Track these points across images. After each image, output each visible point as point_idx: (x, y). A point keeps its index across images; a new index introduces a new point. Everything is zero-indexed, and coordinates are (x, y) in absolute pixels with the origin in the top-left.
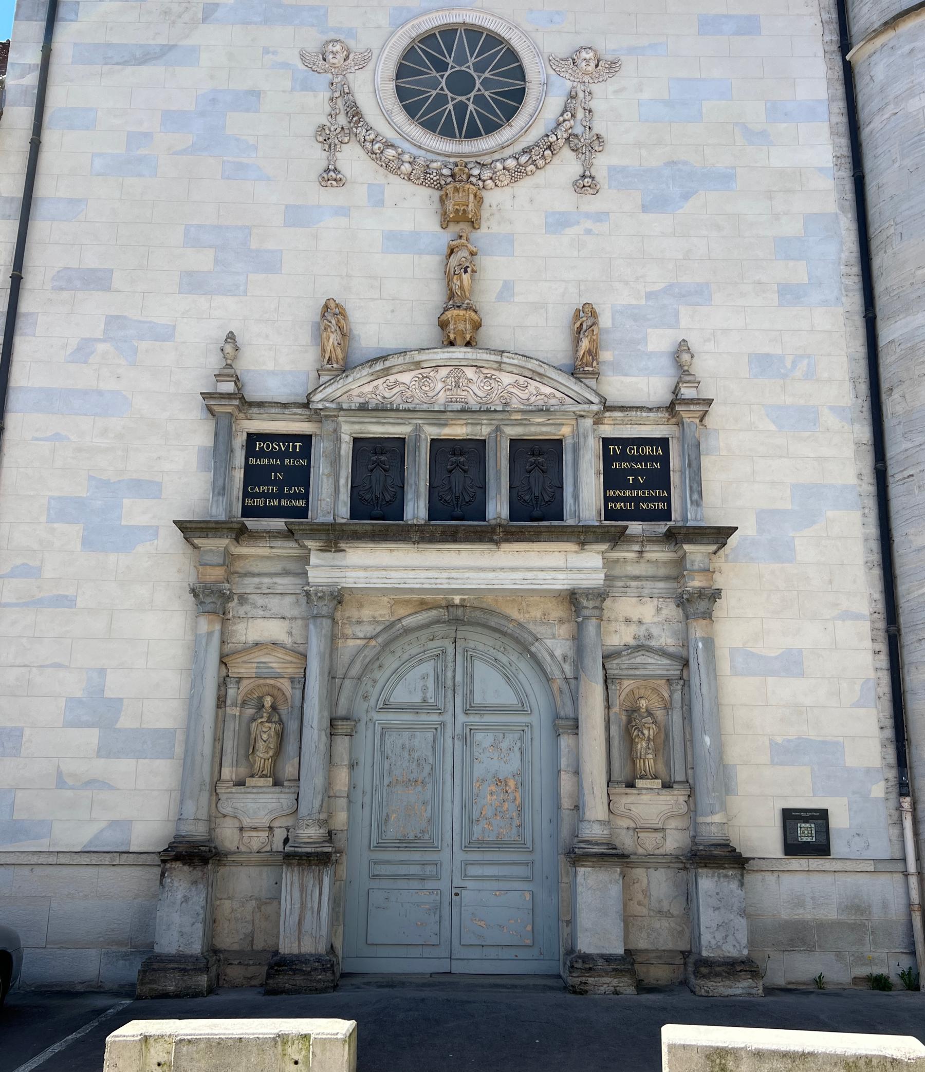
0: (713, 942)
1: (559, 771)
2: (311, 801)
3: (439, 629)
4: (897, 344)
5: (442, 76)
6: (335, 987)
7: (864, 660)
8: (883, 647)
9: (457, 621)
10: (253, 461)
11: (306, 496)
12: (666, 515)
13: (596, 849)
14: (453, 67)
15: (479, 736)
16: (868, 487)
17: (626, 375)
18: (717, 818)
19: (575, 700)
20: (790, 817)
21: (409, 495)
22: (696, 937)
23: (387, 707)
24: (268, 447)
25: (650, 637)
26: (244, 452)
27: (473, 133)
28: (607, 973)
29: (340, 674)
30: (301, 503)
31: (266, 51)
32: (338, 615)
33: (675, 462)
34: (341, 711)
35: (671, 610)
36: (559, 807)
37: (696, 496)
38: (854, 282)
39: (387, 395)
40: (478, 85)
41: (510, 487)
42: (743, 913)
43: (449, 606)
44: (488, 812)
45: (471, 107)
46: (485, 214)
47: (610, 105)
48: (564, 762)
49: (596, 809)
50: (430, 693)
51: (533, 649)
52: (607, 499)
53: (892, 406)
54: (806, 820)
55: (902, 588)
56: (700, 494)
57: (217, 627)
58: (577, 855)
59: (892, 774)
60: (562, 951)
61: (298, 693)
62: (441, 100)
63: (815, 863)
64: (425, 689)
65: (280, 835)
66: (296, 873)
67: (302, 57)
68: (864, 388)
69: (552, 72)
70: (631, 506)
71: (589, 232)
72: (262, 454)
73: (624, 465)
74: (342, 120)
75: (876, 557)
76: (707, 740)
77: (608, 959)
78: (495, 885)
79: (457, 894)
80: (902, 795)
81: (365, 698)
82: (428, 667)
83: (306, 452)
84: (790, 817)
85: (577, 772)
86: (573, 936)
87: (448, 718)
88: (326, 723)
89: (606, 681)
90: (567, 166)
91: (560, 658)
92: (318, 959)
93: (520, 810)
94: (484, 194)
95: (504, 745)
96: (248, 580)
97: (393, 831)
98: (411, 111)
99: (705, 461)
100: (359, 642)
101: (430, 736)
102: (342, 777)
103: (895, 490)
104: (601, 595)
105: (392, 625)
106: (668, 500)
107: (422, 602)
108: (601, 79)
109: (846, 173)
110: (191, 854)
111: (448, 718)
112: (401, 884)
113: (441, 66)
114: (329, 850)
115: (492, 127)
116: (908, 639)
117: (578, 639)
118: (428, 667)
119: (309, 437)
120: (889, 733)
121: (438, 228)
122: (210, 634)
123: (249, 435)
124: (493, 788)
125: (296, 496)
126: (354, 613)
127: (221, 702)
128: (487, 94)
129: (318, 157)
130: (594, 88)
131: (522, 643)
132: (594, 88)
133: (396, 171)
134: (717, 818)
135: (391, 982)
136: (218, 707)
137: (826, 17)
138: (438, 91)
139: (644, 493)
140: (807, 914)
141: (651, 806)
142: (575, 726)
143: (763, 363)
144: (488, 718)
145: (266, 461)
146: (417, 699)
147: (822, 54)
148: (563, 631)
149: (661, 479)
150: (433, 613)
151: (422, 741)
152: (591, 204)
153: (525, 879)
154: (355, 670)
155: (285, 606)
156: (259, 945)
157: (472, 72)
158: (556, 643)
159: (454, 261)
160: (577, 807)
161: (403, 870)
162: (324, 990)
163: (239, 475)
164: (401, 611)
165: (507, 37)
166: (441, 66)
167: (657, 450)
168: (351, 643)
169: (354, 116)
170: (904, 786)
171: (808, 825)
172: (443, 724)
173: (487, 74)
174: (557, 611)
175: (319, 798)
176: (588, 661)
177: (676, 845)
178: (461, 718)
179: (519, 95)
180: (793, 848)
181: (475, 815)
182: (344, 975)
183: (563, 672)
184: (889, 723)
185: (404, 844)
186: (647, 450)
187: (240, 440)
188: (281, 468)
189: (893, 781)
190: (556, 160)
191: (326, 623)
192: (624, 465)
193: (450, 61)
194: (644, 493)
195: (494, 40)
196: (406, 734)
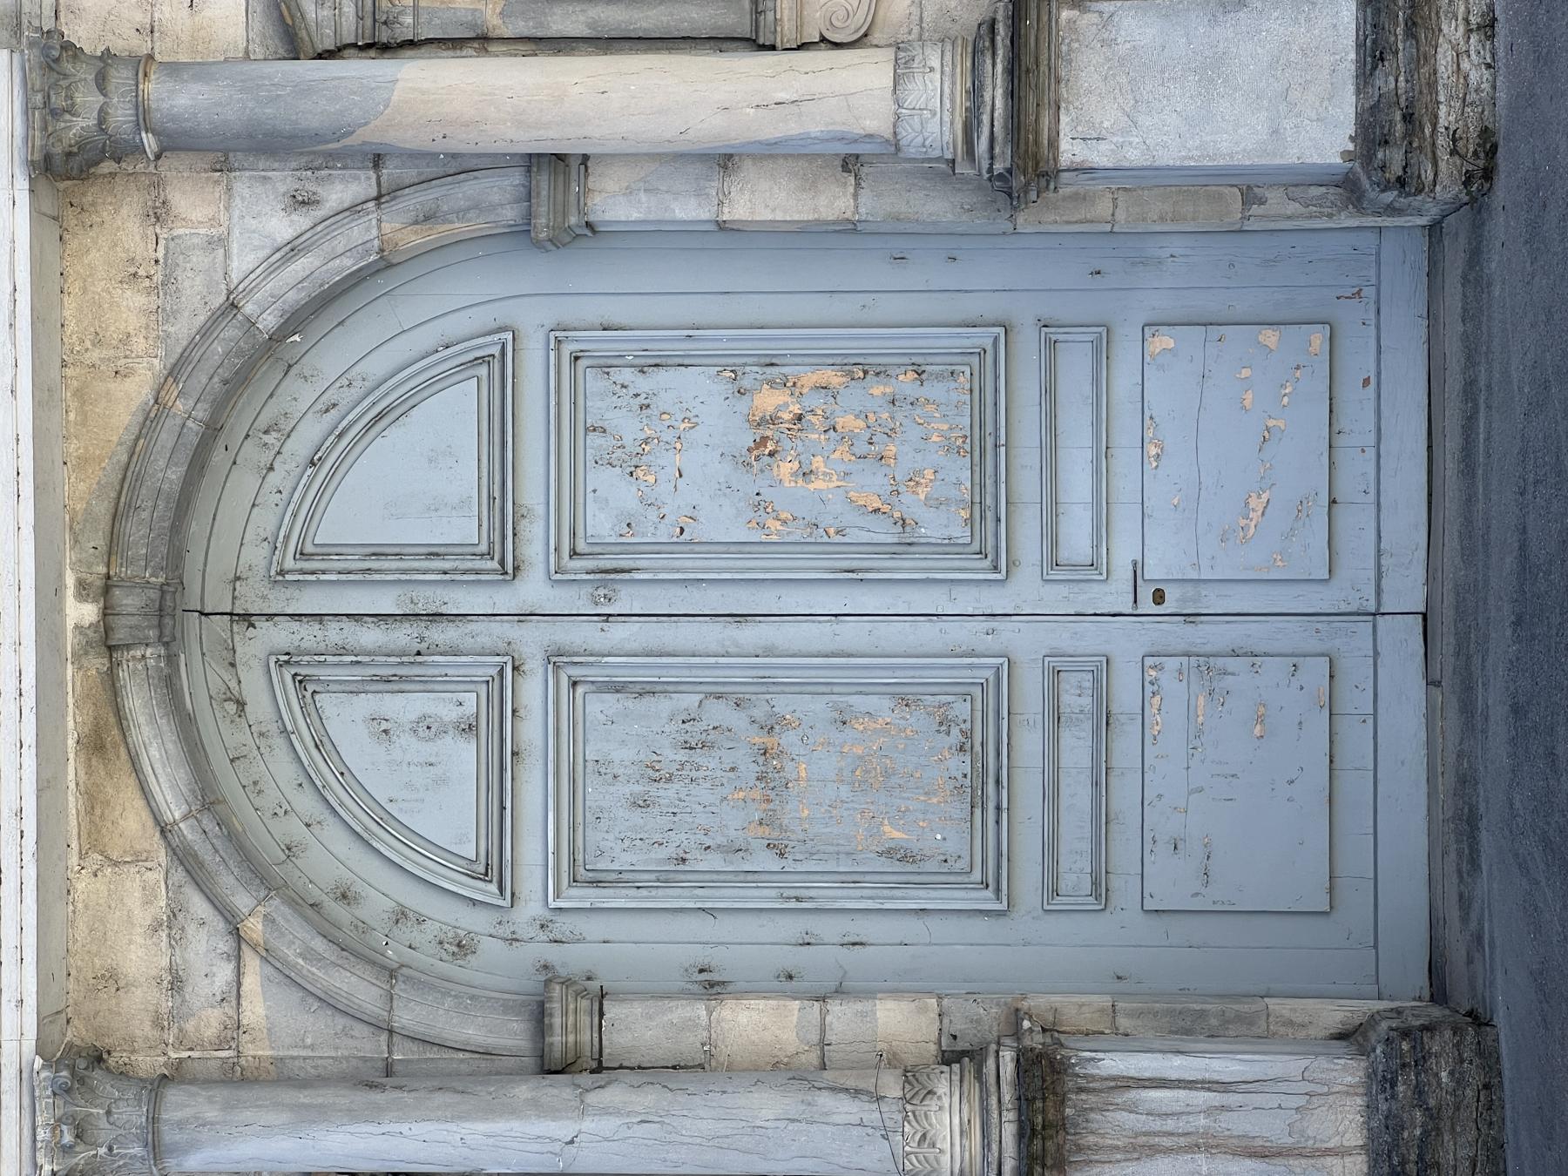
1: (722, 226)
3: (201, 678)
6: (1478, 1020)
9: (168, 614)
13: (996, 95)
15: (600, 524)
19: (461, 166)
23: (494, 868)
28: (1423, 59)
29: (371, 1046)
32: (148, 1063)
34: (513, 1034)
36: (850, 228)
43: (107, 641)
44: (870, 486)
48: (689, 209)
49: (849, 93)
50: (444, 708)
51: (269, 322)
58: (1017, 166)
60: (1348, 220)
64: (426, 727)
78: (1125, 460)
79: (1159, 597)
81: (463, 948)
82: (346, 718)
85: (725, 161)
86: (1297, 181)
87: (532, 641)
88: (558, 1090)
89: (384, 49)
91: (302, 221)
92: (1382, 1083)
93: (862, 369)
95: (629, 428)
97: (942, 831)
100: (251, 982)
101: (599, 706)
102: (751, 1023)
105: (183, 857)
107: (95, 745)
111: (532, 641)
112: (1124, 795)
114: (1008, 1056)
117: (227, 152)
118: (346, 718)
124: (786, 468)
126: (138, 1006)
131: (245, 364)
135: (1459, 825)
142: (555, 169)
144: (532, 492)
146: (463, 757)
148: (194, 204)
150: (138, 701)
151: (621, 735)
153: (1103, 350)
154: (361, 990)
158: (245, 235)
160: (850, 164)
161: (1077, 795)
162: (1489, 1059)
164: (132, 823)
168: (255, 1010)
172: (556, 658)
174: (119, 227)
175: (825, 1100)
176: (313, 114)
178: (533, 590)
181: (885, 533)
182: (1438, 993)
183: (354, 209)
185: (986, 791)
191: (179, 1105)
196: (595, 793)
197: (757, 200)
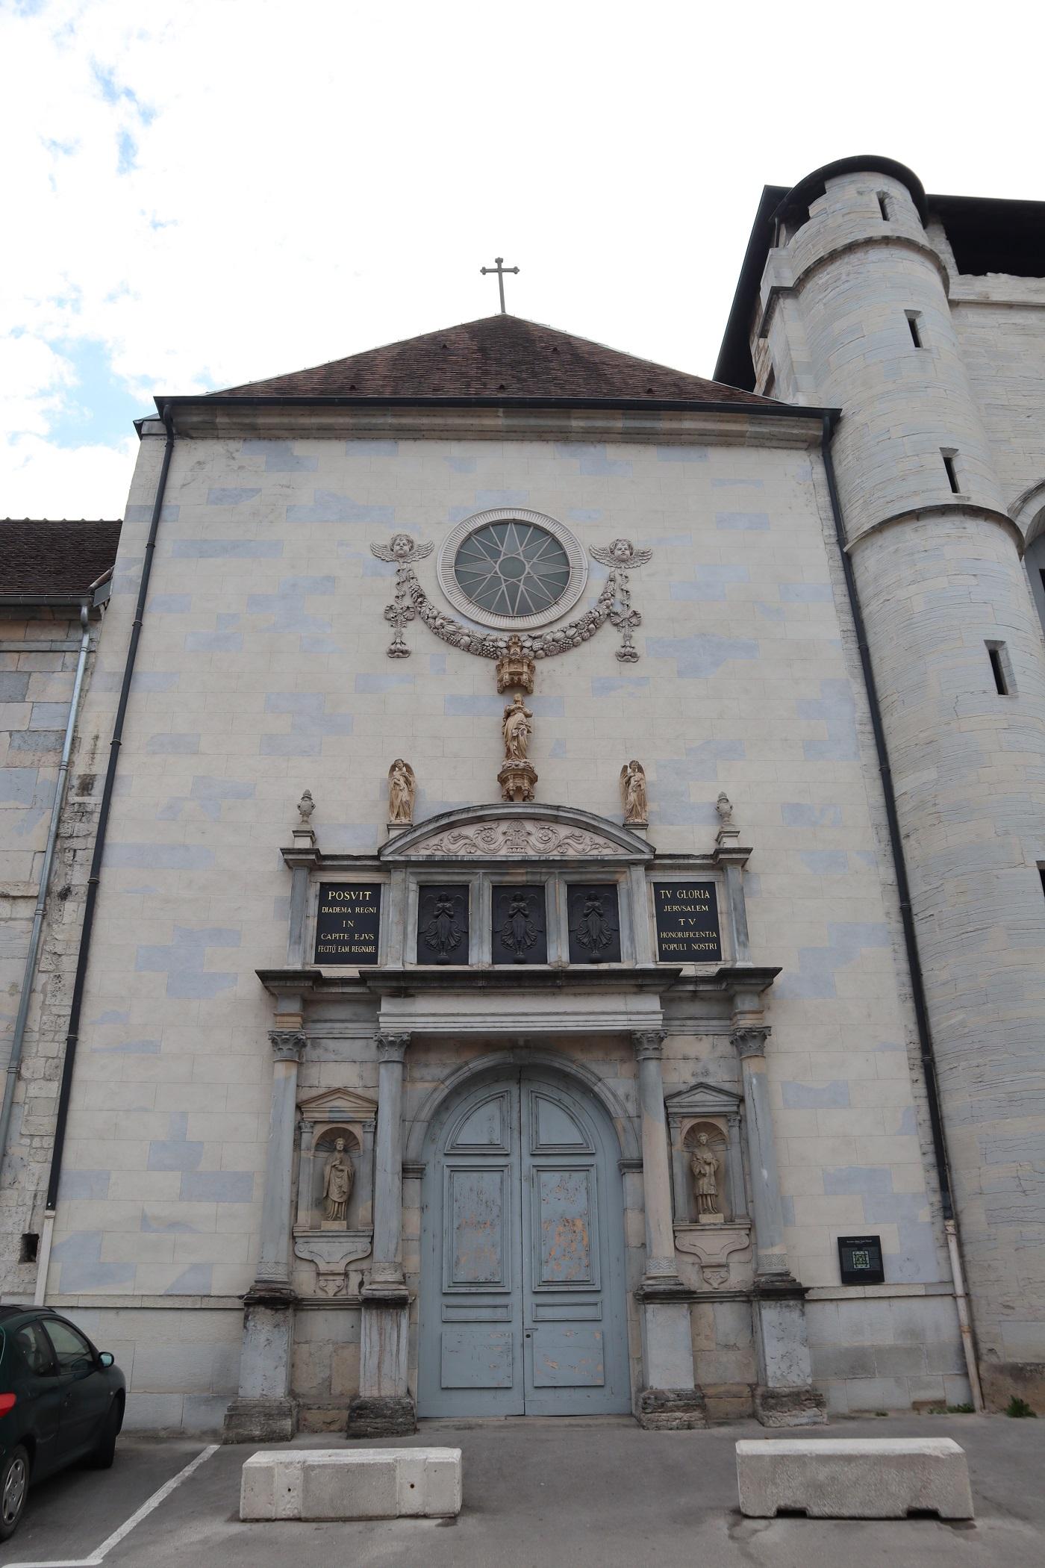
0: (779, 1373)
1: (625, 1210)
2: (385, 1244)
7: (903, 1087)
8: (919, 1074)
10: (325, 910)
11: (375, 943)
12: (716, 955)
16: (897, 926)
18: (776, 1250)
19: (638, 1138)
20: (845, 1244)
21: (474, 941)
22: (762, 1370)
25: (706, 1073)
27: (524, 612)
29: (409, 1116)
30: (370, 949)
33: (722, 905)
35: (724, 1045)
37: (742, 938)
38: (869, 740)
39: (451, 847)
40: (527, 569)
41: (570, 931)
42: (806, 1342)
45: (522, 587)
47: (645, 588)
48: (629, 1201)
49: (663, 1245)
51: (596, 1089)
52: (661, 941)
53: (911, 849)
54: (860, 1248)
55: (934, 1019)
56: (747, 935)
57: (294, 1071)
59: (936, 1198)
60: (633, 1389)
61: (370, 1136)
62: (495, 580)
63: (870, 1290)
65: (355, 1279)
66: (374, 1317)
67: (373, 549)
68: (885, 833)
72: (334, 903)
73: (675, 908)
74: (408, 602)
75: (908, 990)
76: (765, 1173)
77: (679, 1396)
80: (946, 1218)
83: (375, 901)
84: (845, 1244)
86: (643, 1374)
89: (667, 1118)
90: (609, 639)
91: (622, 1097)
94: (535, 663)
96: (319, 1025)
98: (468, 591)
99: (750, 904)
100: (427, 1085)
103: (920, 928)
104: (659, 1038)
106: (717, 941)
109: (853, 646)
110: (271, 1300)
114: (406, 1293)
115: (542, 606)
116: (942, 1067)
119: (379, 885)
120: (931, 1158)
121: (496, 693)
122: (287, 1079)
124: (561, 1229)
125: (366, 943)
127: (297, 1144)
129: (385, 634)
130: (628, 572)
132: (628, 572)
133: (456, 644)
134: (776, 1250)
136: (295, 1150)
137: (823, 515)
140: (866, 1341)
141: (713, 1243)
142: (638, 1166)
147: (822, 546)
149: (710, 921)
156: (337, 1389)
159: (513, 721)
160: (644, 1245)
163: (313, 923)
166: (495, 554)
170: (948, 1210)
175: (395, 1241)
180: (850, 1277)
181: (544, 1257)
183: (626, 1111)
184: (931, 1148)
186: (696, 893)
188: (352, 916)
189: (938, 1205)
190: (600, 633)
192: (675, 908)
193: (503, 549)
197: (633, 1219)
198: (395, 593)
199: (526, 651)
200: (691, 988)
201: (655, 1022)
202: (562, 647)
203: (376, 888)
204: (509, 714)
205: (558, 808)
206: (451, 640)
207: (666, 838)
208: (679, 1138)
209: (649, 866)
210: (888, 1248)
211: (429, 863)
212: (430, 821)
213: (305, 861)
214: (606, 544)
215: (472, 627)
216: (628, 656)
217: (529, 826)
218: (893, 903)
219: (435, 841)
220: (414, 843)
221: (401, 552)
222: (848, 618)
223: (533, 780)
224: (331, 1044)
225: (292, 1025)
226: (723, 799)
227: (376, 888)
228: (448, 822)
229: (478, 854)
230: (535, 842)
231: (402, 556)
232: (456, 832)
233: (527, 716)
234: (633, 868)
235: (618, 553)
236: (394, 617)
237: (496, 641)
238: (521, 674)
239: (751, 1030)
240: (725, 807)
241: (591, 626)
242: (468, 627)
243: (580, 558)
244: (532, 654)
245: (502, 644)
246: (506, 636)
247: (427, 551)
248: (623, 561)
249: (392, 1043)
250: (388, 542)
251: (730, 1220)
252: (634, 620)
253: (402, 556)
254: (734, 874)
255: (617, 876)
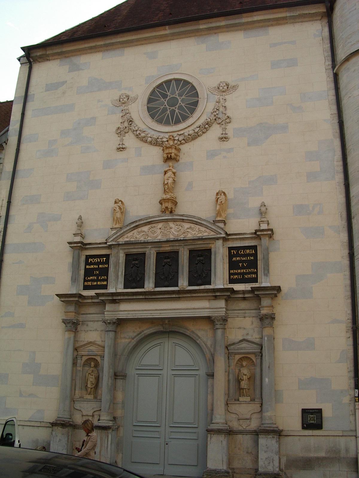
4: (355, 197)
5: (165, 100)
10: (88, 267)
11: (107, 280)
12: (255, 280)
14: (170, 96)
17: (239, 219)
24: (93, 260)
26: (84, 263)
27: (178, 122)
30: (105, 283)
31: (99, 101)
33: (259, 256)
35: (256, 322)
36: (207, 409)
37: (266, 272)
39: (138, 236)
40: (180, 102)
41: (189, 271)
45: (177, 111)
46: (181, 155)
51: (198, 342)
52: (230, 274)
54: (312, 414)
62: (165, 110)
69: (210, 93)
70: (240, 277)
71: (225, 157)
72: (91, 264)
73: (238, 259)
74: (126, 124)
75: (349, 293)
79: (167, 444)
83: (107, 262)
90: (215, 131)
98: (152, 116)
100: (126, 340)
102: (120, 396)
108: (230, 93)
113: (165, 96)
115: (185, 118)
121: (163, 163)
123: (86, 256)
125: (103, 280)
128: (183, 105)
129: (115, 141)
130: (226, 97)
132: (226, 97)
133: (146, 142)
137: (326, 54)
138: (164, 106)
139: (246, 271)
141: (245, 408)
143: (300, 209)
145: (92, 266)
147: (324, 70)
149: (254, 264)
152: (226, 145)
155: (99, 325)
157: (177, 97)
163: (82, 272)
165: (191, 82)
166: (165, 96)
167: (252, 251)
168: (123, 341)
169: (130, 122)
171: (313, 416)
173: (183, 97)
177: (256, 425)
179: (196, 104)
180: (306, 426)
186: (248, 251)
187: (83, 258)
190: (211, 128)
192: (238, 259)
193: (168, 94)
194: (246, 271)
195: (186, 83)
198: (121, 121)
199: (176, 142)
200: (241, 296)
201: (222, 313)
202: (195, 137)
203: (107, 256)
204: (165, 172)
205: (182, 215)
206: (144, 140)
207: (233, 227)
208: (233, 363)
209: (225, 239)
210: (326, 414)
211: (127, 244)
212: (127, 226)
213: (79, 246)
214: (216, 85)
215: (153, 132)
216: (224, 138)
217: (171, 224)
218: (346, 252)
219: (131, 234)
220: (122, 235)
221: (124, 101)
222: (334, 107)
223: (175, 203)
224: (90, 324)
225: (72, 316)
226: (263, 205)
227: (107, 256)
228: (137, 225)
229: (150, 239)
230: (175, 231)
231: (123, 103)
232: (140, 229)
233: (174, 173)
234: (217, 241)
235: (221, 88)
236: (120, 132)
237: (161, 139)
238: (171, 153)
239: (266, 315)
240: (263, 209)
241: (208, 125)
242: (151, 133)
243: (202, 93)
244: (179, 143)
245: (165, 140)
246: (167, 136)
247: (136, 99)
248: (224, 92)
249: (109, 323)
250: (118, 98)
251: (253, 400)
252: (228, 120)
253: (123, 103)
254: (265, 241)
255: (210, 245)
